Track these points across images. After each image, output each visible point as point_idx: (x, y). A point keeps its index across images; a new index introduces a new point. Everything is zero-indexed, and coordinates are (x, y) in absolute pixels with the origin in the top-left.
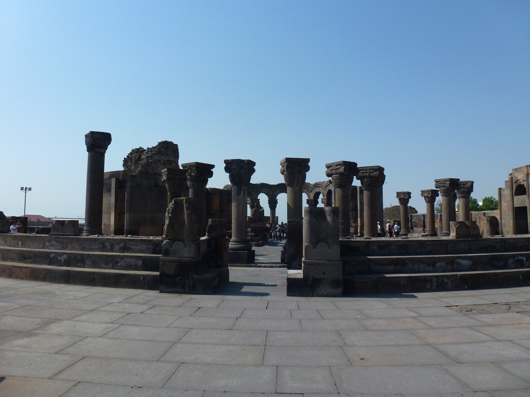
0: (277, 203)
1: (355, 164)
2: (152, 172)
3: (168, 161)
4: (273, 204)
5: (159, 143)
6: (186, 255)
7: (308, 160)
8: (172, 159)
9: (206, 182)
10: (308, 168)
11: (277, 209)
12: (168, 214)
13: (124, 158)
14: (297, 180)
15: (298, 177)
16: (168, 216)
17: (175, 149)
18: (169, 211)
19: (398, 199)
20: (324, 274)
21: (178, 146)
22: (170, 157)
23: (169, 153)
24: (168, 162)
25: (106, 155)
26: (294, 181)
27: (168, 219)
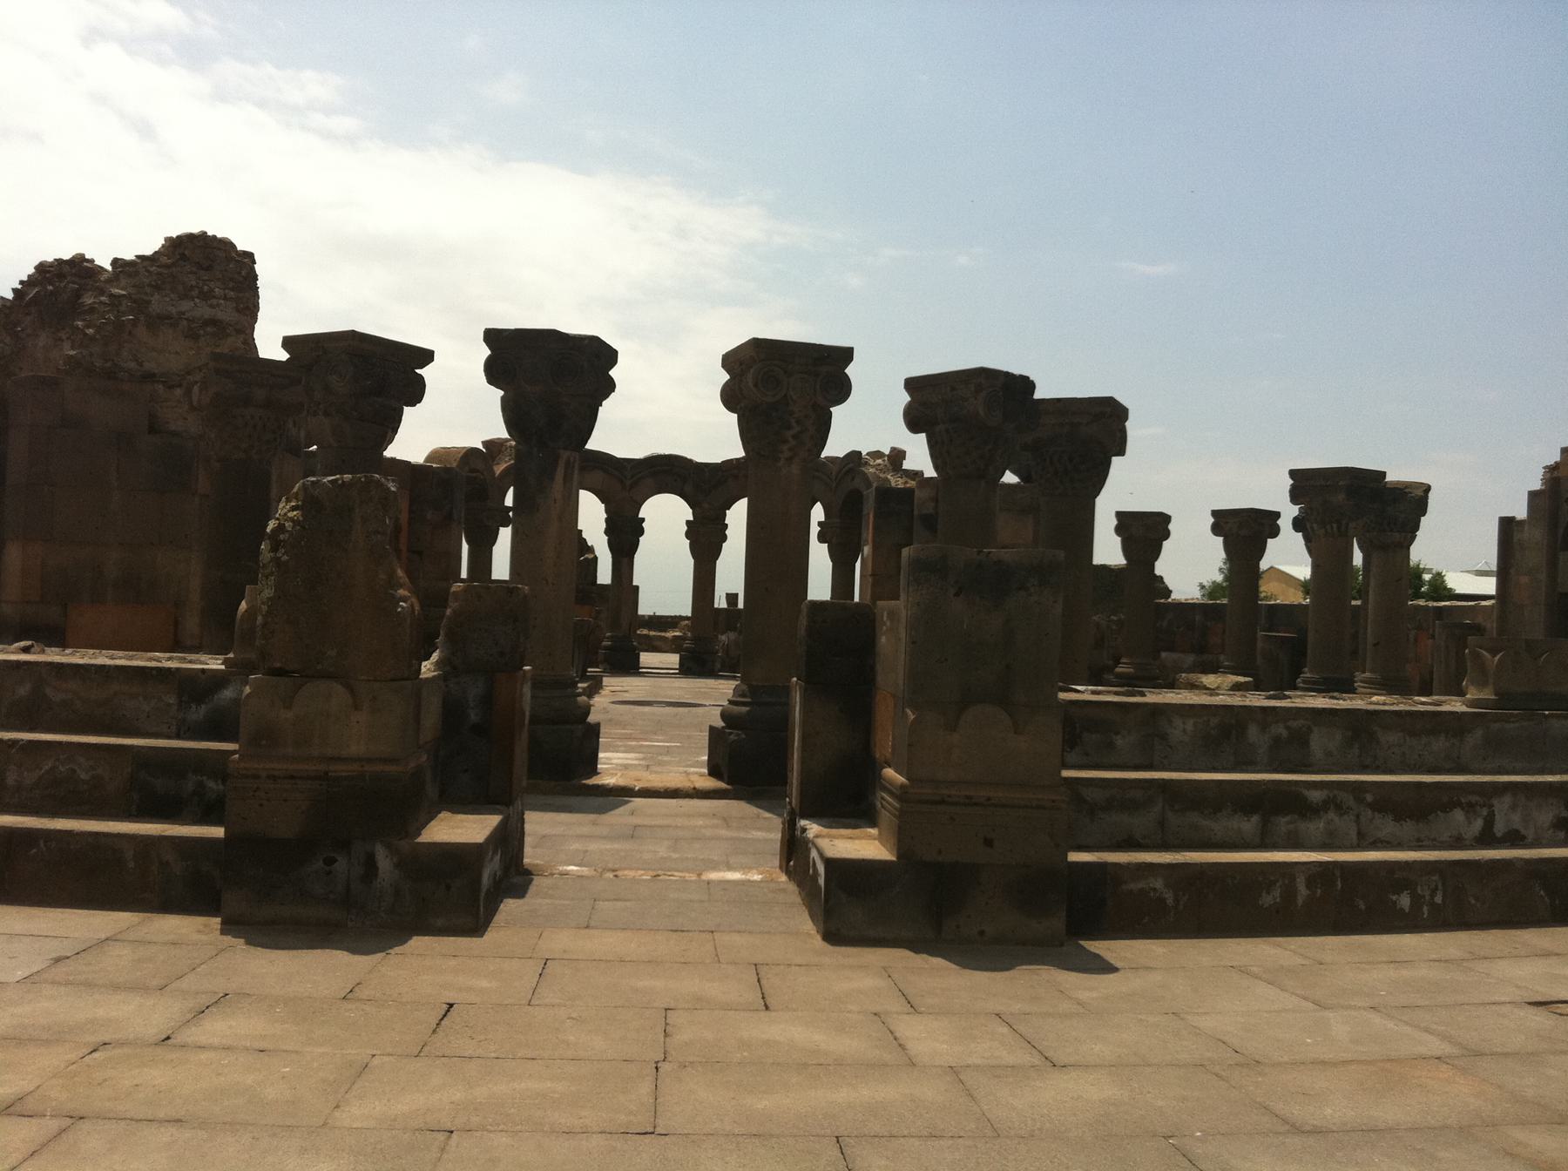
0: (641, 532)
2: (133, 365)
3: (213, 322)
5: (167, 239)
6: (356, 749)
7: (846, 355)
8: (226, 313)
10: (842, 390)
11: (639, 558)
12: (274, 549)
15: (798, 422)
16: (277, 561)
17: (243, 273)
18: (282, 537)
20: (989, 843)
21: (254, 262)
23: (212, 290)
26: (785, 441)
27: (272, 574)
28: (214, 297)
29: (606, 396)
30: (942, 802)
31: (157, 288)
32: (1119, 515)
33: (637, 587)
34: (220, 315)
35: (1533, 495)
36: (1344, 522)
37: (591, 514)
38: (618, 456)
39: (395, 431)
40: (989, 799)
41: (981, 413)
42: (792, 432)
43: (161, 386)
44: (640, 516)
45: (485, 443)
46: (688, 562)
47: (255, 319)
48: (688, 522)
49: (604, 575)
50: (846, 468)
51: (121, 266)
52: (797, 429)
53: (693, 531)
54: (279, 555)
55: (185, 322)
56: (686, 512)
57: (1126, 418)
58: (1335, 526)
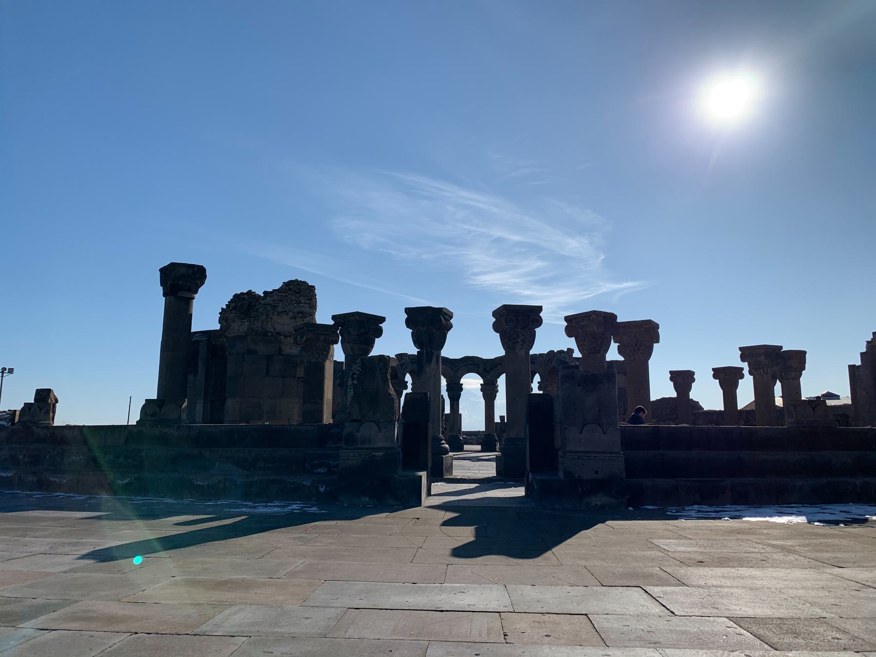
1: (613, 317)
2: (272, 330)
4: (455, 391)
8: (307, 309)
9: (371, 344)
12: (353, 380)
13: (222, 308)
14: (522, 341)
18: (355, 376)
19: (672, 383)
20: (597, 472)
22: (303, 306)
23: (300, 301)
24: (300, 315)
26: (518, 342)
28: (301, 303)
33: (461, 414)
34: (304, 309)
35: (862, 355)
36: (765, 369)
38: (451, 358)
40: (595, 457)
42: (520, 339)
43: (283, 337)
48: (481, 385)
49: (447, 410)
53: (483, 388)
58: (762, 370)
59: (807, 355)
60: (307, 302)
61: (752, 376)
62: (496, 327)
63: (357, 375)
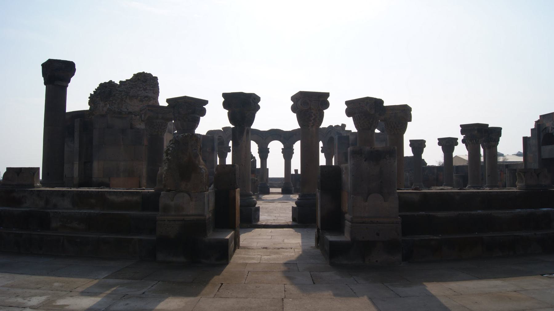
0: (269, 152)
1: (380, 102)
3: (147, 97)
4: (264, 153)
7: (327, 95)
10: (326, 105)
11: (268, 160)
12: (167, 156)
13: (91, 94)
14: (313, 119)
15: (314, 115)
16: (168, 159)
17: (155, 83)
18: (169, 152)
20: (378, 234)
23: (146, 88)
24: (146, 99)
25: (69, 89)
26: (311, 121)
27: (166, 163)
28: (147, 90)
29: (257, 110)
30: (363, 223)
31: (132, 88)
32: (410, 141)
33: (268, 169)
36: (477, 140)
37: (254, 148)
39: (198, 124)
41: (368, 110)
42: (313, 118)
43: (134, 116)
44: (268, 147)
45: (223, 128)
46: (283, 161)
47: (158, 95)
48: (282, 149)
49: (258, 166)
50: (328, 131)
51: (122, 83)
52: (314, 117)
54: (168, 157)
55: (139, 97)
56: (282, 146)
57: (411, 111)
58: (475, 141)
59: (502, 130)
60: (152, 89)
61: (464, 144)
62: (294, 109)
63: (170, 151)
